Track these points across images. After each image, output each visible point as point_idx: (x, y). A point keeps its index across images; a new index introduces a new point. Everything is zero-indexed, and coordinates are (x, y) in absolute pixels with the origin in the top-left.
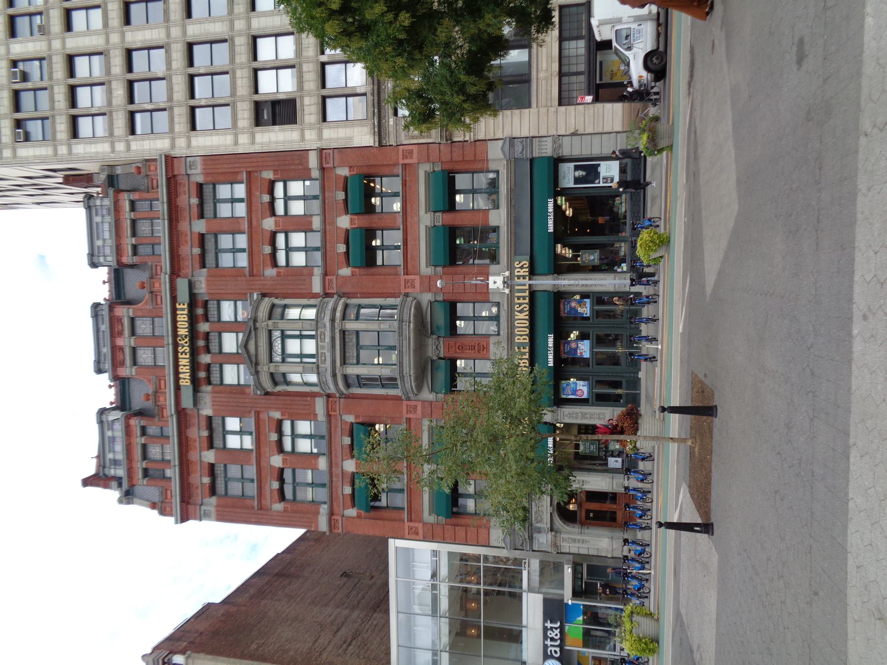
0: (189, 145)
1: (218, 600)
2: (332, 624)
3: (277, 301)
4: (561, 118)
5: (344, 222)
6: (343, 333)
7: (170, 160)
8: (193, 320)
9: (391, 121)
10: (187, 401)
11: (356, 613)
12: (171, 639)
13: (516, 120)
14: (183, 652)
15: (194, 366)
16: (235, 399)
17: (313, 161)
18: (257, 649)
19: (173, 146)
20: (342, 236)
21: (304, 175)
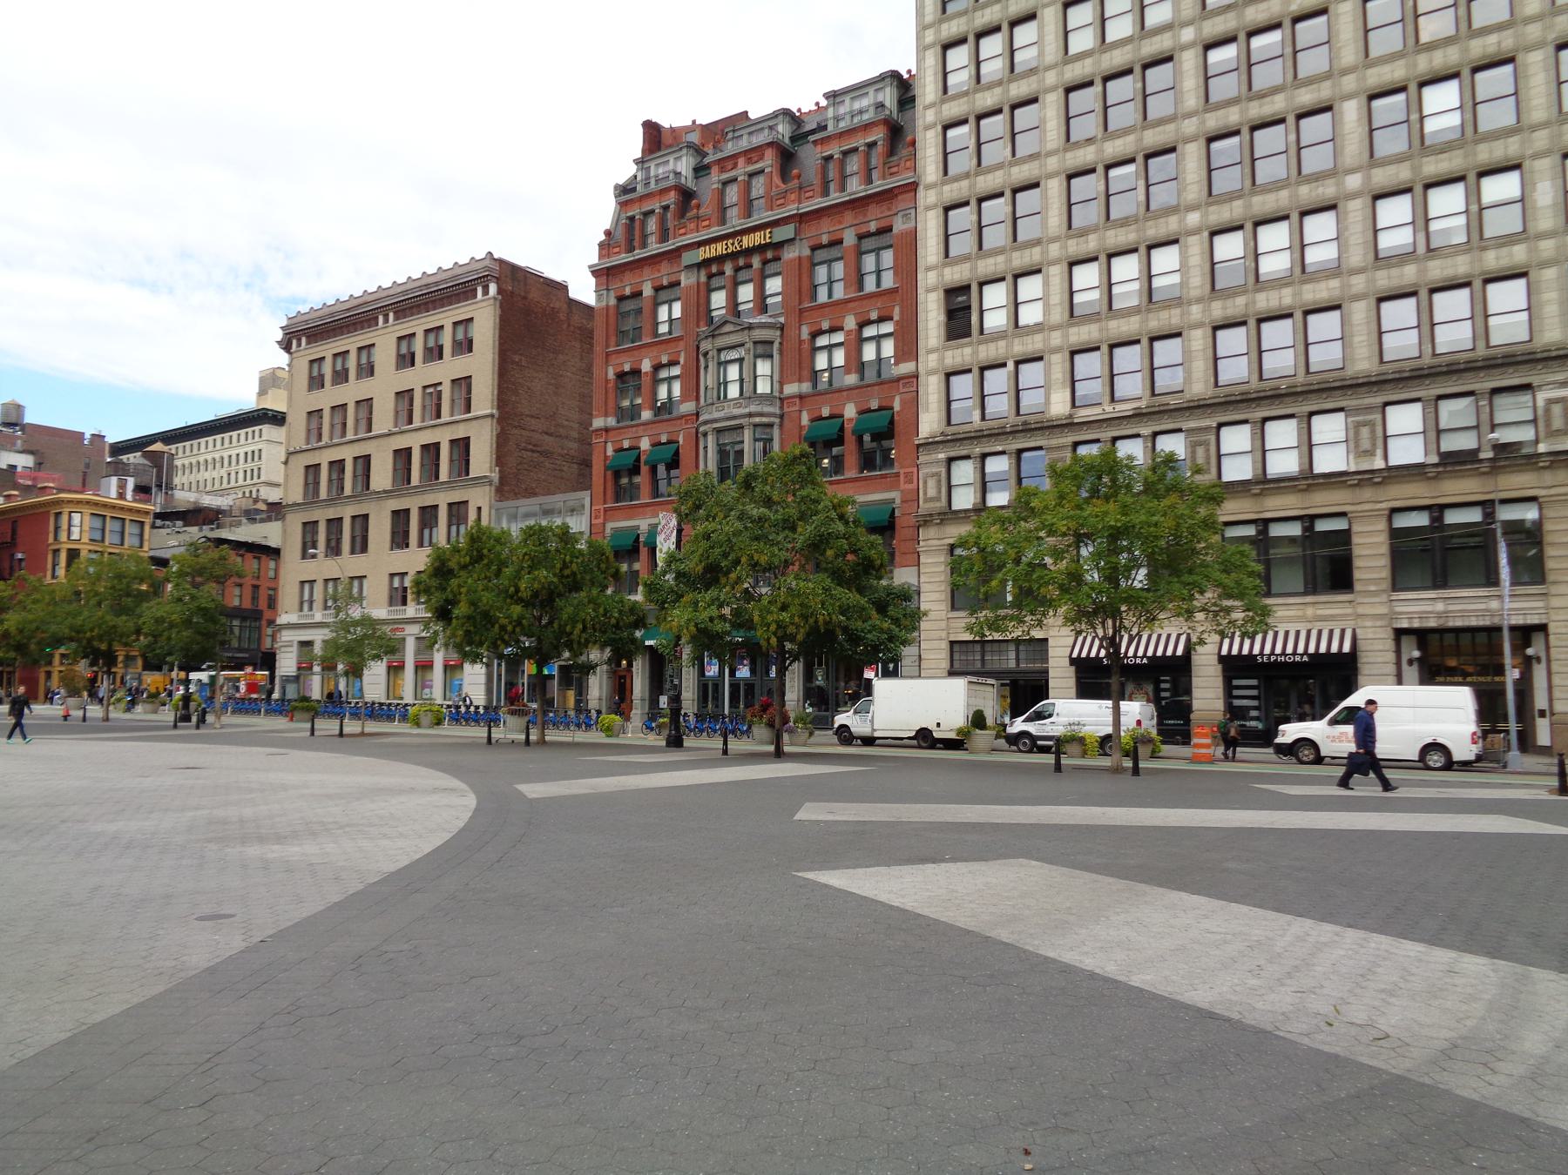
0: (928, 208)
1: (572, 294)
2: (557, 425)
3: (776, 346)
4: (936, 644)
5: (850, 411)
6: (741, 427)
7: (913, 187)
8: (761, 249)
9: (942, 456)
10: (689, 258)
11: (574, 445)
12: (514, 269)
13: (936, 596)
14: (500, 291)
15: (720, 259)
16: (699, 309)
17: (906, 368)
18: (513, 362)
19: (928, 187)
20: (836, 412)
21: (900, 356)
